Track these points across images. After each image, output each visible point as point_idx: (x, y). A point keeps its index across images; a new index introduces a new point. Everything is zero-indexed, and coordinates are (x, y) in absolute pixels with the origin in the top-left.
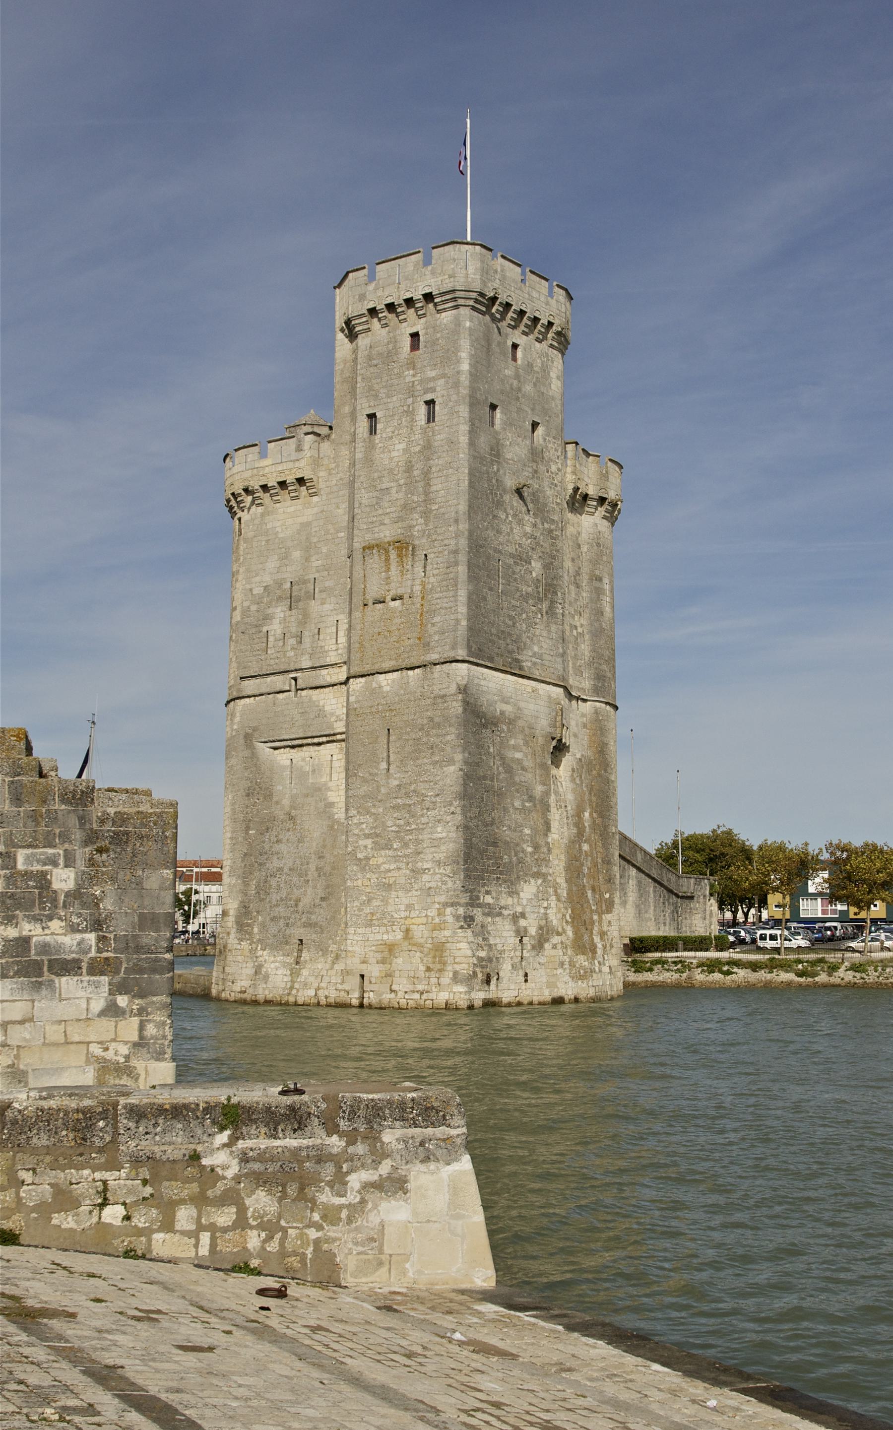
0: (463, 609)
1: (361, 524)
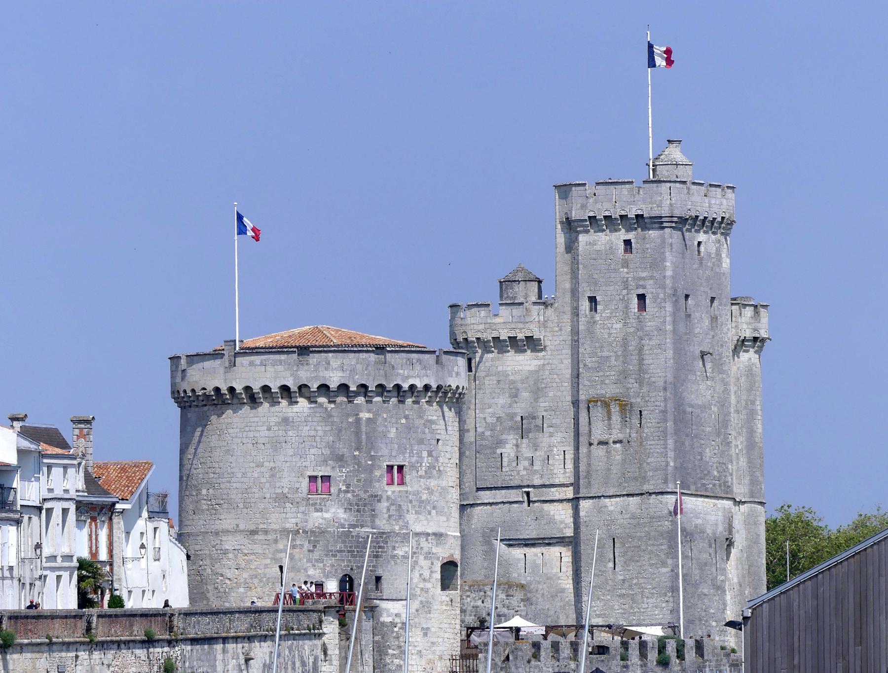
1: (584, 382)
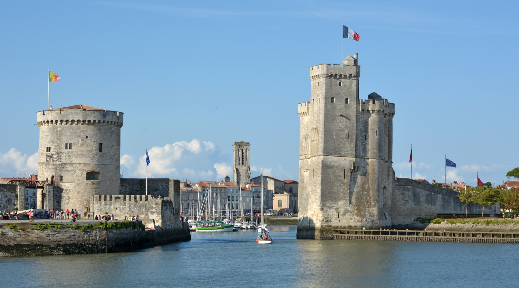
0: (323, 144)
